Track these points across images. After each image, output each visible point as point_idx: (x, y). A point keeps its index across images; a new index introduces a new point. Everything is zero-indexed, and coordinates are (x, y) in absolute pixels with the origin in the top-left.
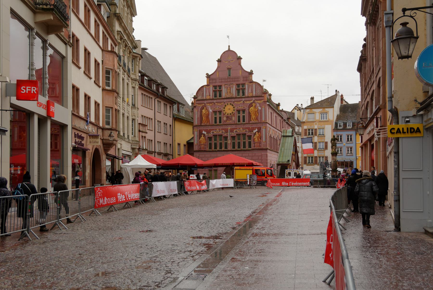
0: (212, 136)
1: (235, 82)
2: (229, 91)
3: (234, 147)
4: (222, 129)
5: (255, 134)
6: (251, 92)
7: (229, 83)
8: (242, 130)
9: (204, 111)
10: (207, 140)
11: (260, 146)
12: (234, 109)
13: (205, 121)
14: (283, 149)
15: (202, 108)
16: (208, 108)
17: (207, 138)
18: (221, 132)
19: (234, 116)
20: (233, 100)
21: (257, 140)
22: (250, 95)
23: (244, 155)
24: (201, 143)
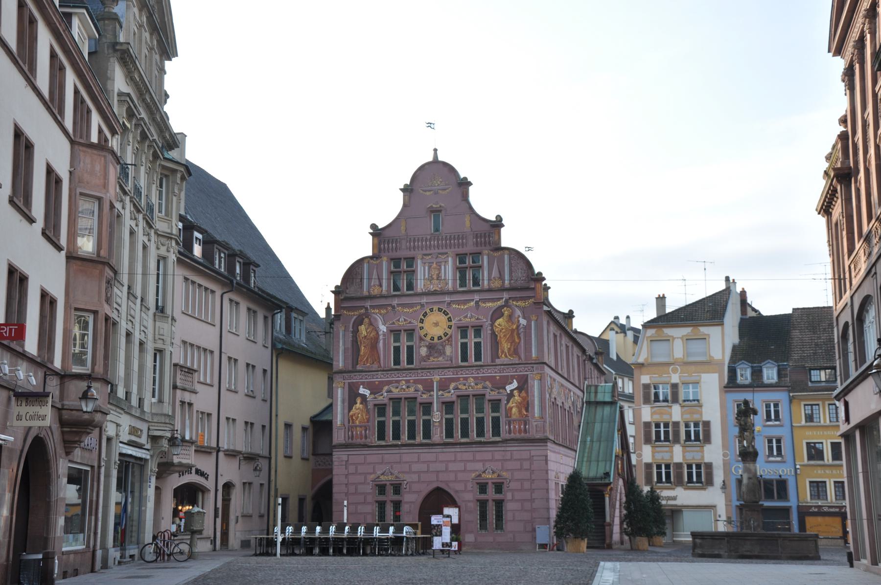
0: (386, 401)
1: (453, 250)
2: (434, 273)
3: (450, 433)
4: (416, 382)
5: (511, 395)
6: (498, 276)
7: (437, 251)
8: (472, 384)
9: (362, 328)
10: (371, 413)
11: (525, 431)
12: (450, 323)
13: (367, 359)
14: (589, 439)
15: (359, 322)
16: (376, 320)
17: (370, 406)
18: (412, 389)
20: (447, 299)
21: (517, 414)
22: (497, 284)
23: (479, 456)
24: (353, 422)
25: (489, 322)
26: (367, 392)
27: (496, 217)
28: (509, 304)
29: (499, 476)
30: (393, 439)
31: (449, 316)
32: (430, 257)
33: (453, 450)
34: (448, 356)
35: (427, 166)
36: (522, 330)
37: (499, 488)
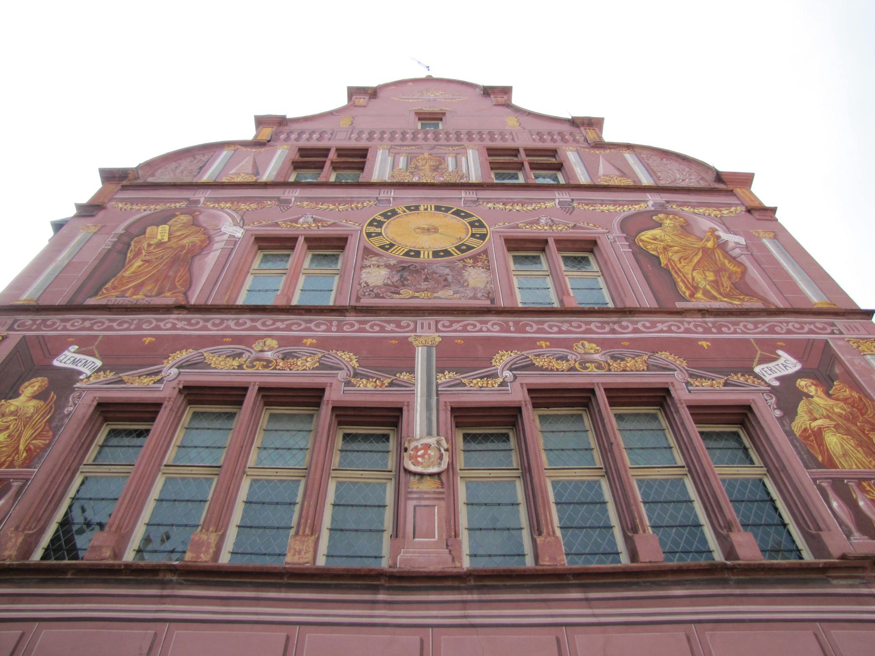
34: (475, 289)
35: (411, 84)
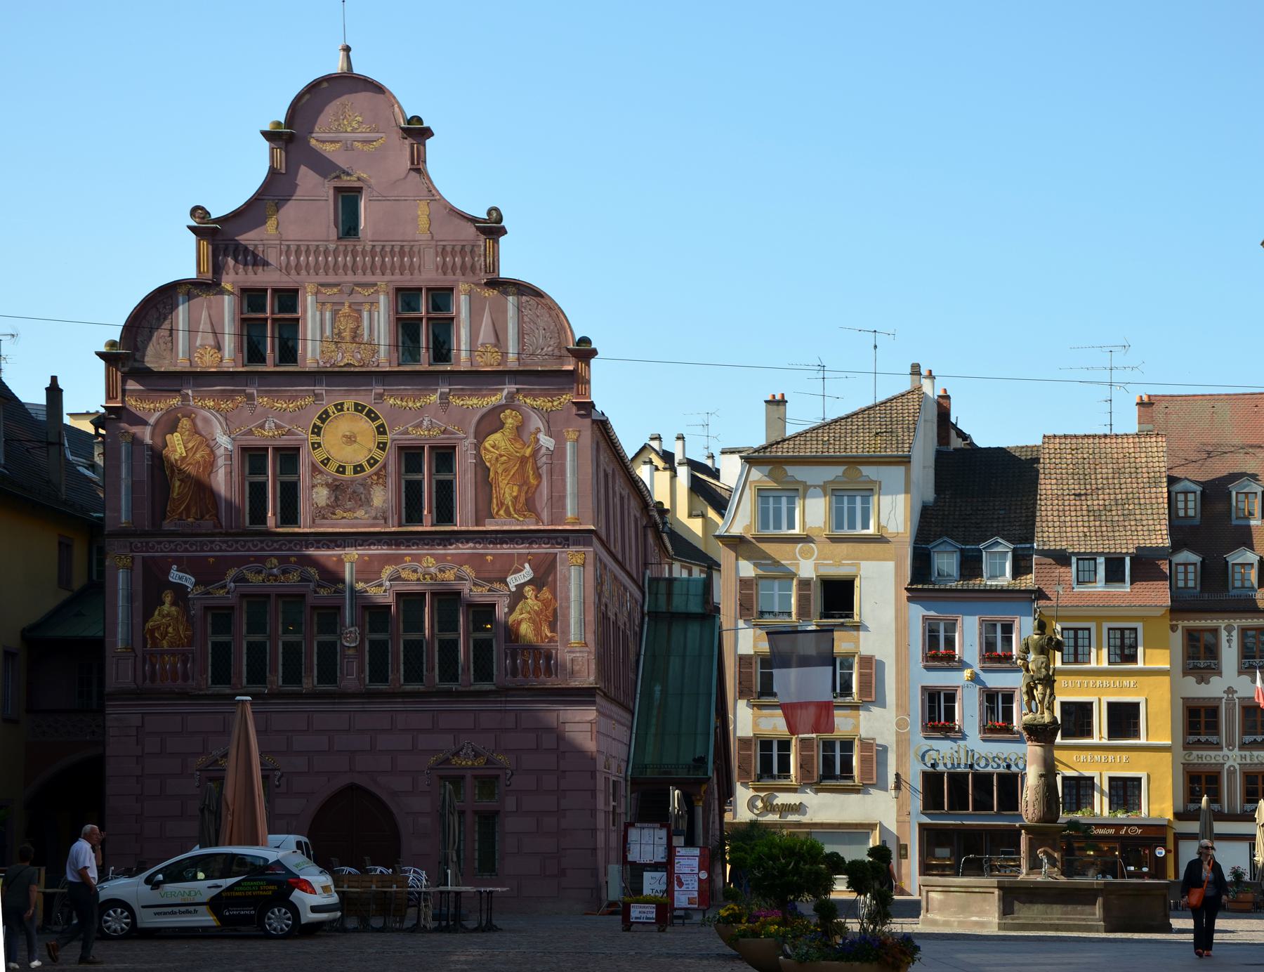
0: (232, 600)
1: (388, 278)
2: (346, 326)
3: (379, 671)
5: (517, 596)
6: (493, 340)
7: (350, 278)
12: (382, 438)
13: (188, 508)
17: (196, 610)
18: (294, 577)
19: (385, 485)
25: (472, 440)
26: (188, 581)
27: (489, 213)
28: (516, 402)
29: (488, 762)
30: (248, 682)
31: (378, 422)
32: (335, 290)
33: (387, 707)
34: (376, 508)
36: (544, 459)
37: (488, 783)
